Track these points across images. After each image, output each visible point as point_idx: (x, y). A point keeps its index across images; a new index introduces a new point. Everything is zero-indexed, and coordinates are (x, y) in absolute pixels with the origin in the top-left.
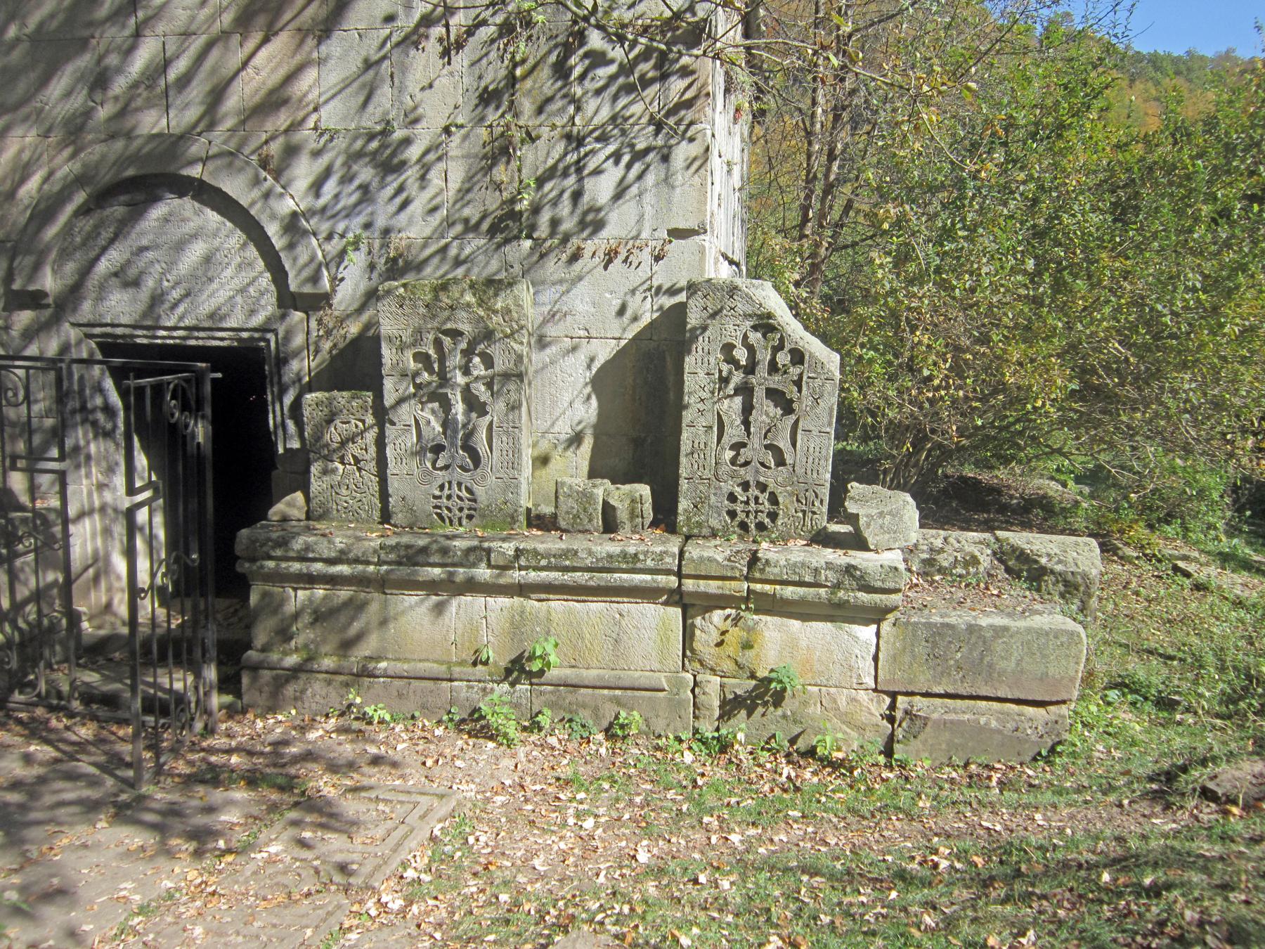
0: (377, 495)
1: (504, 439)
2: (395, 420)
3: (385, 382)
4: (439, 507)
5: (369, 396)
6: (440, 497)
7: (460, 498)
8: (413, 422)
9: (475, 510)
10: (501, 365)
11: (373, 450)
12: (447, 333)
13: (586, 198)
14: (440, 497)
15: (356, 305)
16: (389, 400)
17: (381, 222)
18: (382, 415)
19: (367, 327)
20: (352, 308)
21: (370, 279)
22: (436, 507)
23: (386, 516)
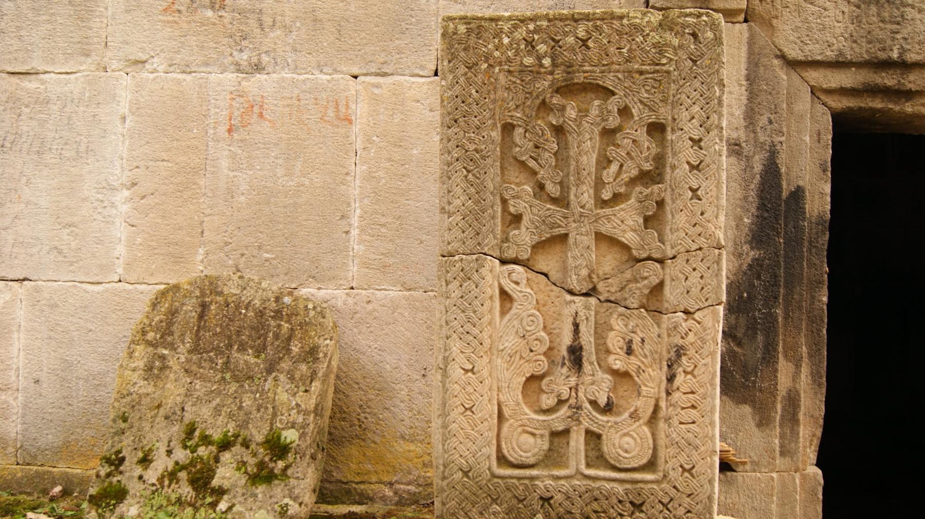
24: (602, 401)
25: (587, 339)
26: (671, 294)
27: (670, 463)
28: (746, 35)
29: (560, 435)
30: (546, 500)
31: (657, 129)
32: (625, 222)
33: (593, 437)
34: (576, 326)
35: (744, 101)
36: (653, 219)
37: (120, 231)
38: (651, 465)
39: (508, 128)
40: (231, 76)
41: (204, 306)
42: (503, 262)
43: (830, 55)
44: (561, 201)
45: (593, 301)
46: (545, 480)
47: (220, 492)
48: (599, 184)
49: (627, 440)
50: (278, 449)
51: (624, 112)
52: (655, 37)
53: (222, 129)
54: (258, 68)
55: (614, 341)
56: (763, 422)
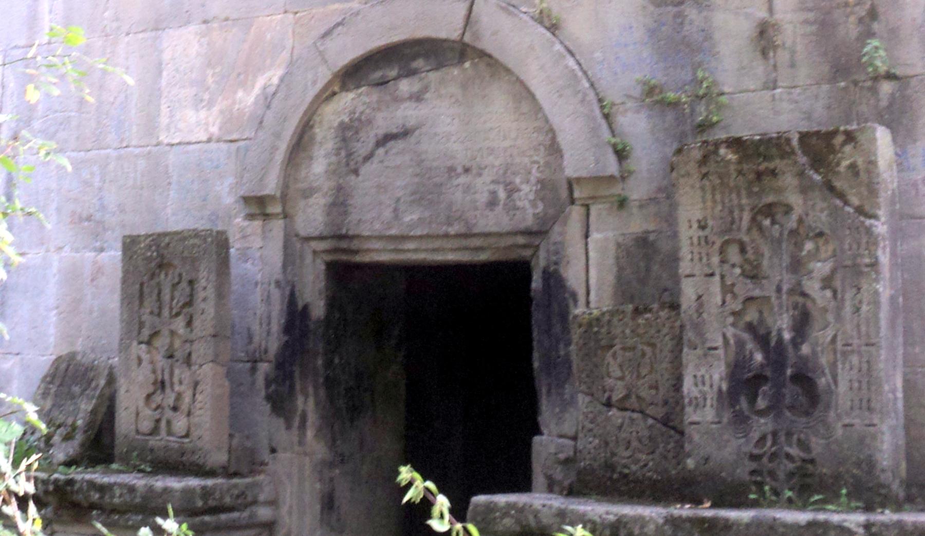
24: (172, 405)
25: (167, 377)
26: (194, 356)
27: (195, 433)
28: (283, 226)
29: (158, 421)
30: (152, 450)
31: (191, 282)
32: (179, 325)
33: (169, 423)
34: (163, 371)
35: (282, 258)
36: (189, 323)
37: (52, 330)
38: (187, 436)
39: (142, 285)
40: (93, 254)
41: (68, 366)
42: (141, 343)
43: (317, 233)
44: (159, 315)
45: (170, 360)
46: (153, 442)
47: (52, 446)
48: (171, 309)
49: (180, 424)
50: (74, 428)
51: (180, 275)
52: (192, 241)
53: (89, 280)
54: (102, 250)
55: (176, 380)
56: (289, 427)
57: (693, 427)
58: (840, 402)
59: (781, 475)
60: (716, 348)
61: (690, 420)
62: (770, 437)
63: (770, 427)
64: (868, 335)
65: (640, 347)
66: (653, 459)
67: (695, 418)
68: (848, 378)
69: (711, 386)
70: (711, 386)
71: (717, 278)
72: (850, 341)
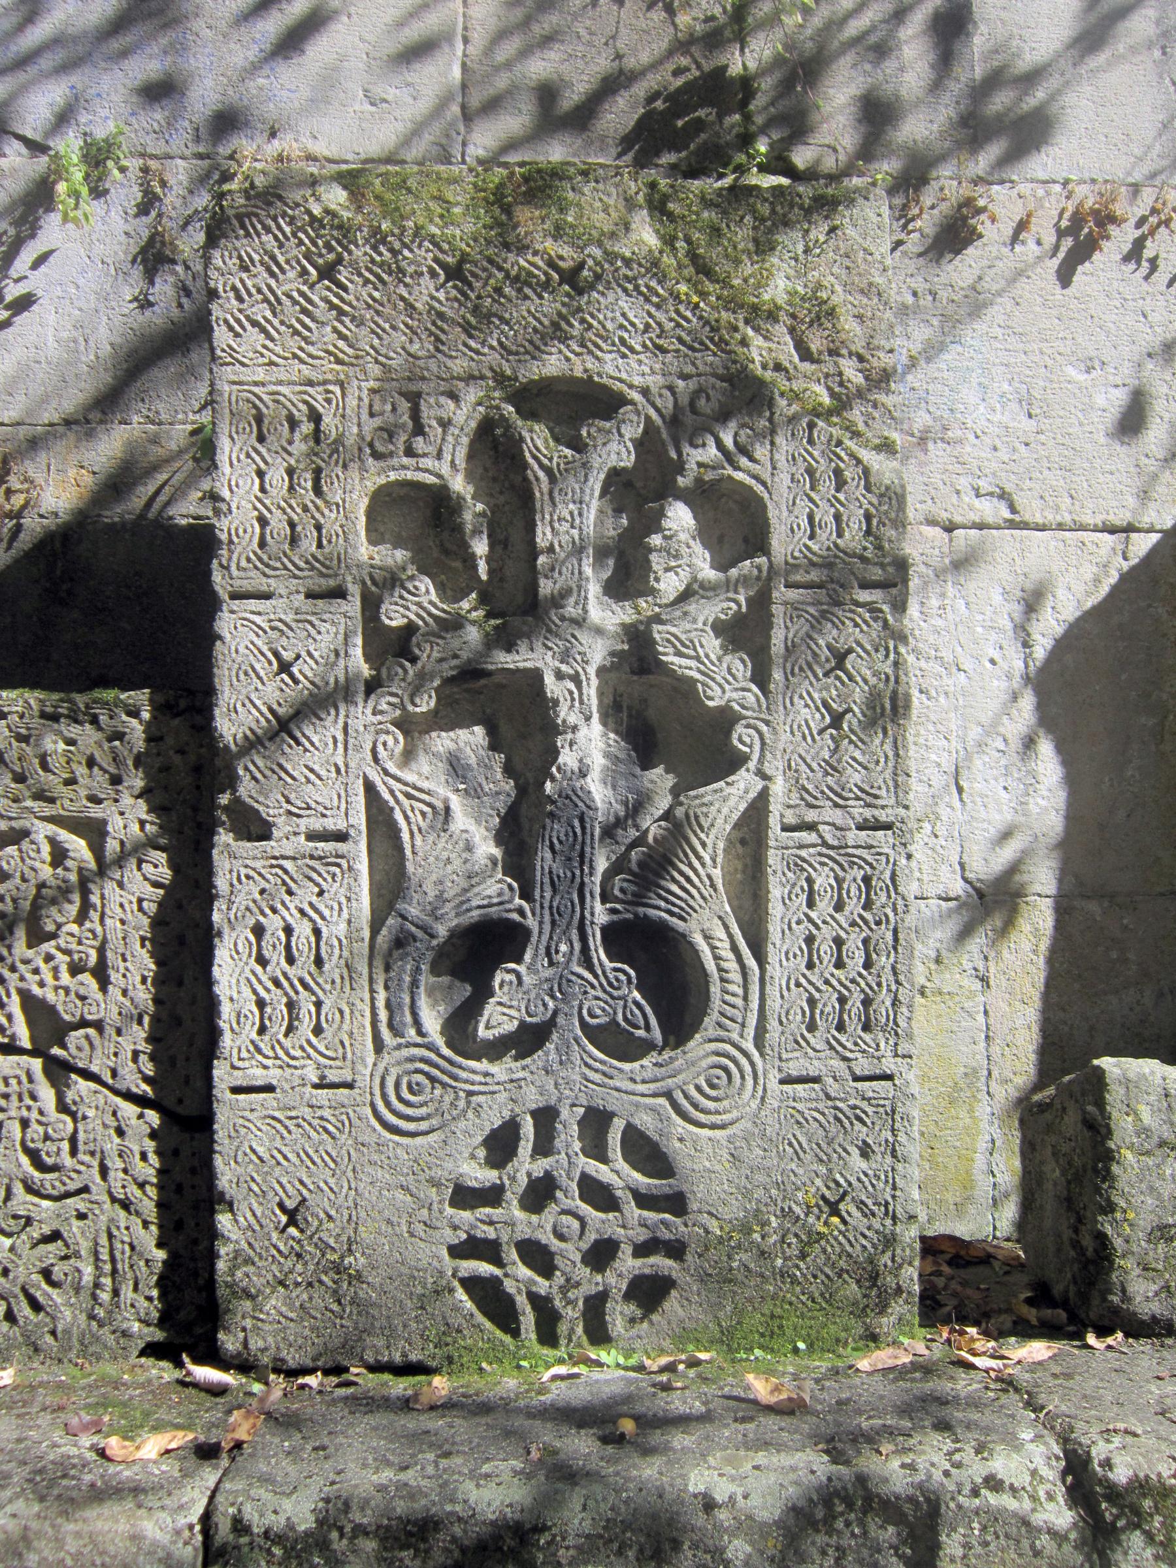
0: (149, 1208)
1: (823, 880)
2: (271, 808)
3: (225, 623)
4: (488, 1250)
5: (134, 713)
6: (492, 1196)
7: (598, 1194)
8: (360, 819)
9: (676, 1250)
10: (793, 527)
11: (136, 968)
12: (535, 399)
13: (979, 42)
14: (492, 1196)
15: (72, 400)
16: (240, 705)
17: (205, 95)
18: (195, 793)
19: (117, 484)
20: (49, 415)
21: (144, 303)
22: (473, 1248)
23: (191, 1315)
57: (242, 1097)
58: (774, 1004)
59: (570, 1254)
60: (341, 837)
61: (239, 1079)
62: (528, 1128)
63: (532, 1098)
64: (869, 797)
65: (42, 831)
66: (82, 1216)
67: (259, 1076)
68: (801, 930)
69: (319, 962)
70: (319, 962)
71: (353, 606)
72: (811, 816)
